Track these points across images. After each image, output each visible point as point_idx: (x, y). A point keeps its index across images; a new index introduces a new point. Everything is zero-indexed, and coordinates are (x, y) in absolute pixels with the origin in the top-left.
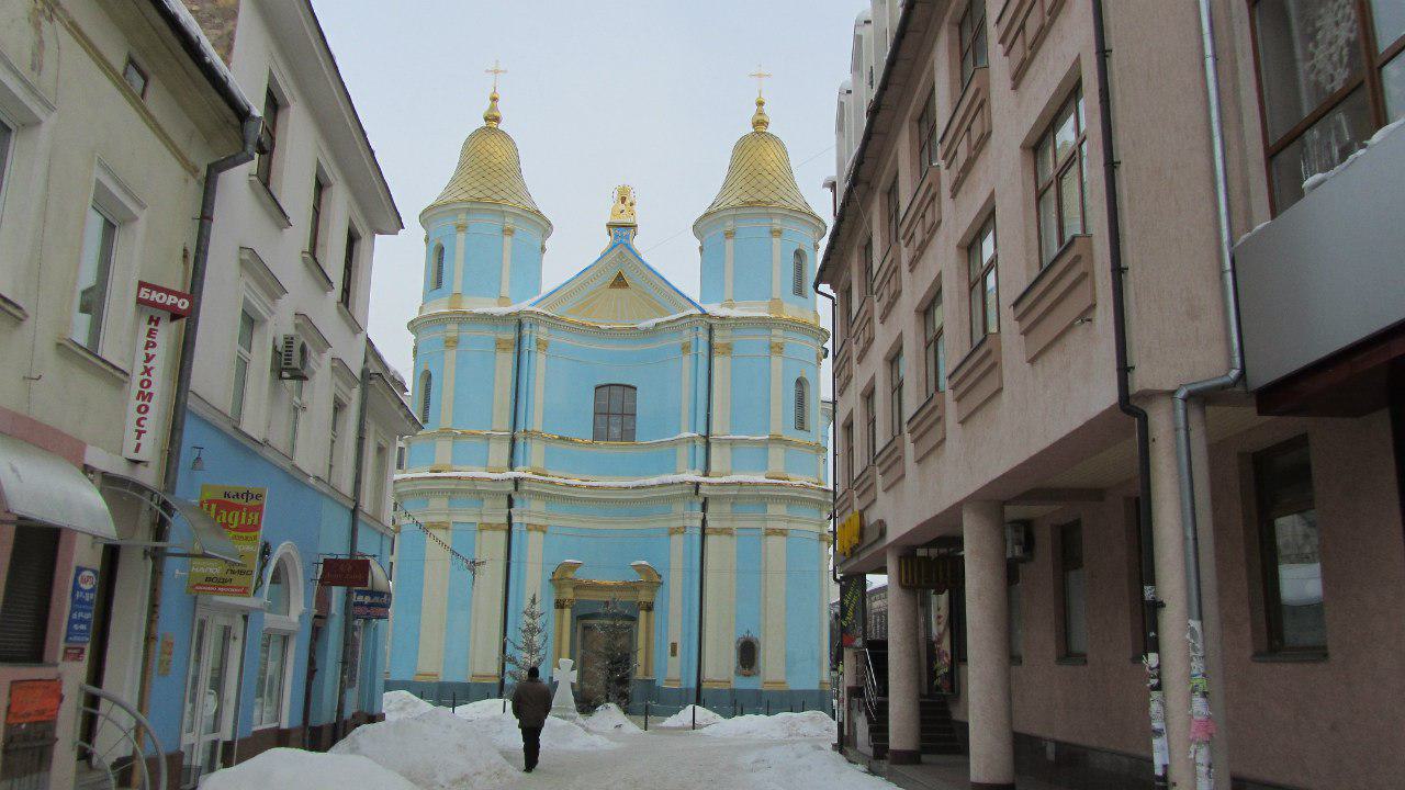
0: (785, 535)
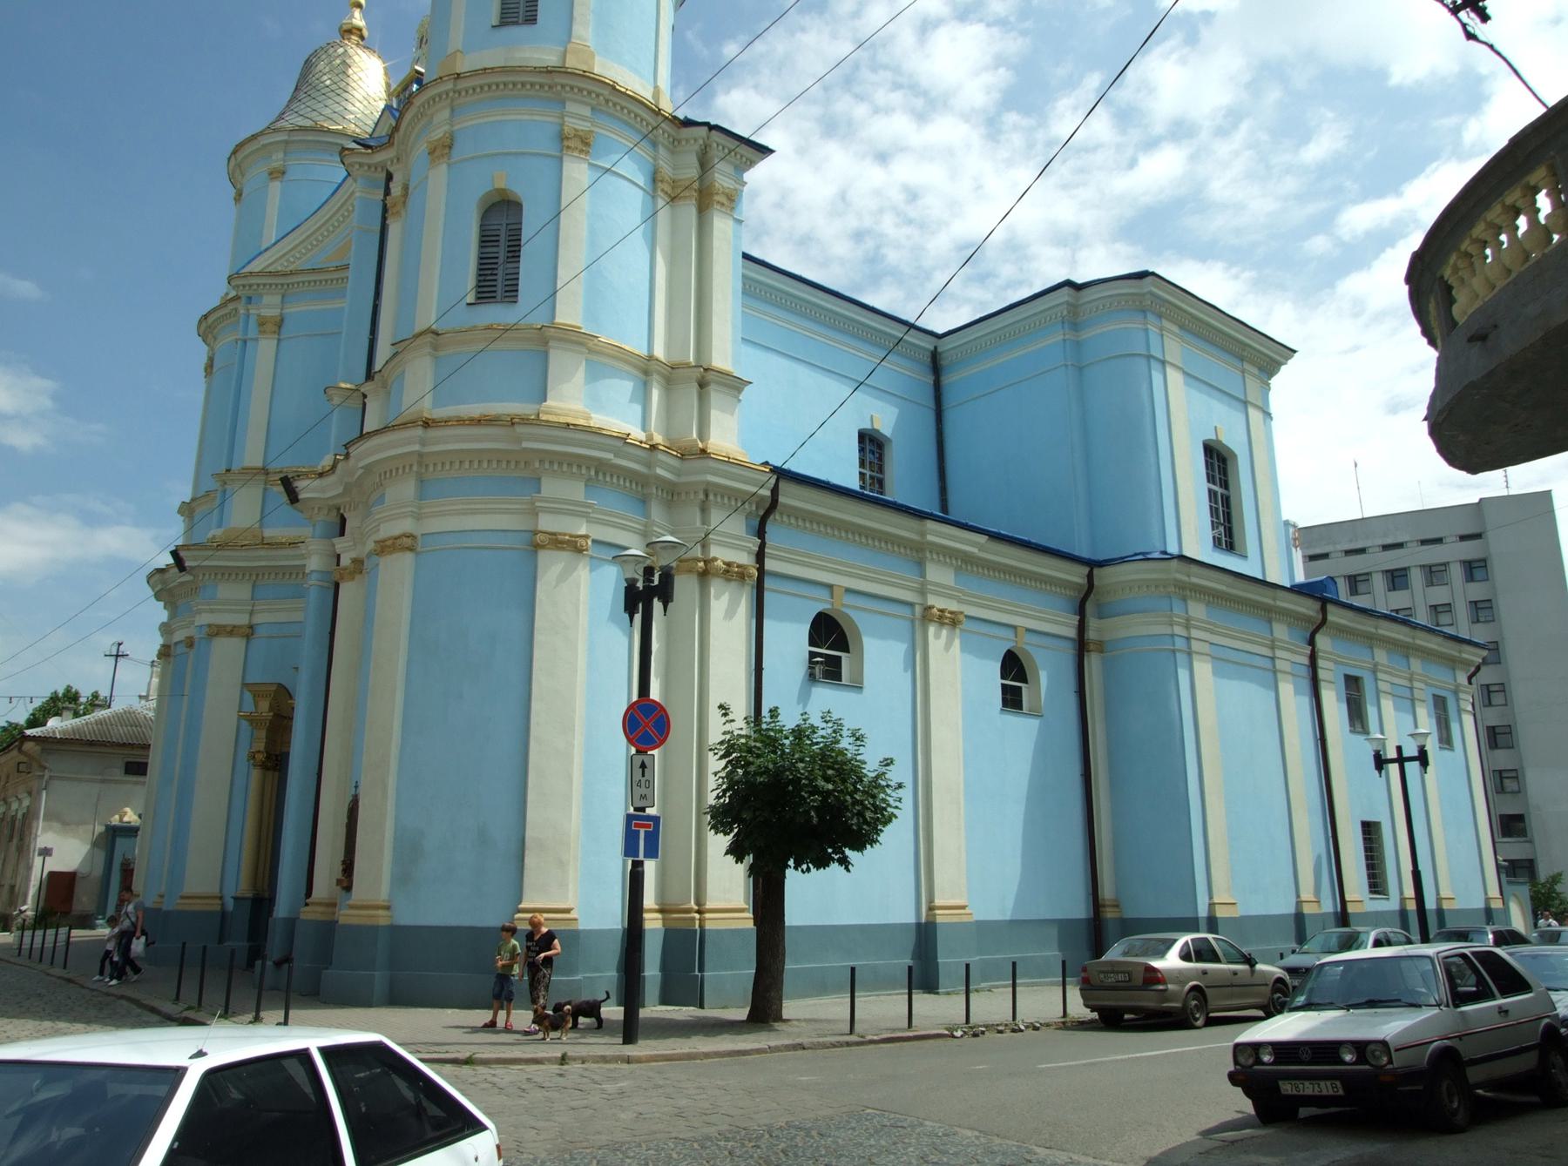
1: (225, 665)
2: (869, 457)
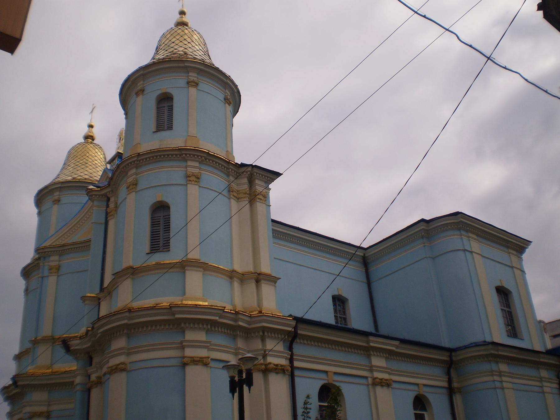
0: (206, 365)
2: (338, 308)
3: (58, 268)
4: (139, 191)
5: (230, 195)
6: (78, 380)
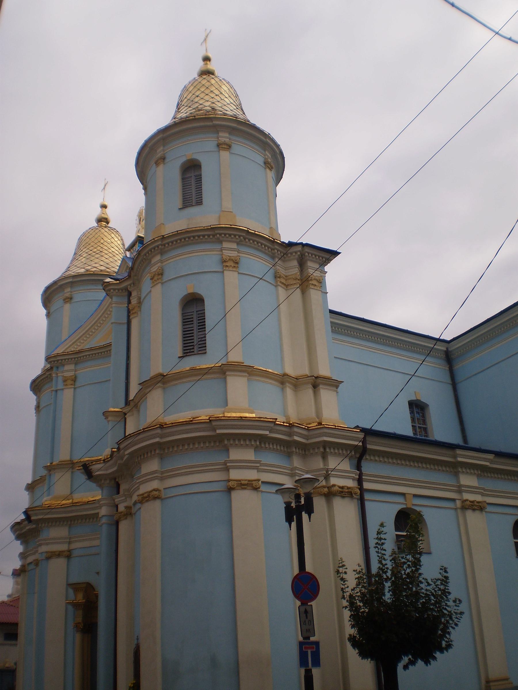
0: (256, 489)
1: (57, 573)
2: (416, 415)
3: (74, 379)
4: (166, 282)
5: (276, 282)
6: (103, 511)
